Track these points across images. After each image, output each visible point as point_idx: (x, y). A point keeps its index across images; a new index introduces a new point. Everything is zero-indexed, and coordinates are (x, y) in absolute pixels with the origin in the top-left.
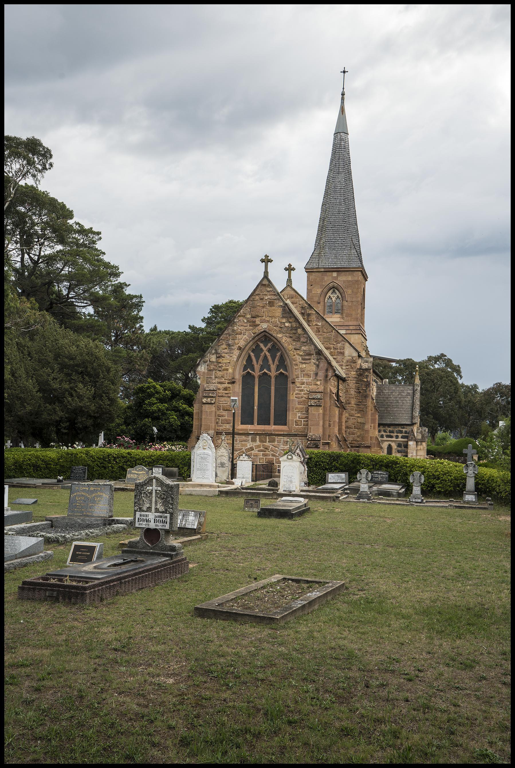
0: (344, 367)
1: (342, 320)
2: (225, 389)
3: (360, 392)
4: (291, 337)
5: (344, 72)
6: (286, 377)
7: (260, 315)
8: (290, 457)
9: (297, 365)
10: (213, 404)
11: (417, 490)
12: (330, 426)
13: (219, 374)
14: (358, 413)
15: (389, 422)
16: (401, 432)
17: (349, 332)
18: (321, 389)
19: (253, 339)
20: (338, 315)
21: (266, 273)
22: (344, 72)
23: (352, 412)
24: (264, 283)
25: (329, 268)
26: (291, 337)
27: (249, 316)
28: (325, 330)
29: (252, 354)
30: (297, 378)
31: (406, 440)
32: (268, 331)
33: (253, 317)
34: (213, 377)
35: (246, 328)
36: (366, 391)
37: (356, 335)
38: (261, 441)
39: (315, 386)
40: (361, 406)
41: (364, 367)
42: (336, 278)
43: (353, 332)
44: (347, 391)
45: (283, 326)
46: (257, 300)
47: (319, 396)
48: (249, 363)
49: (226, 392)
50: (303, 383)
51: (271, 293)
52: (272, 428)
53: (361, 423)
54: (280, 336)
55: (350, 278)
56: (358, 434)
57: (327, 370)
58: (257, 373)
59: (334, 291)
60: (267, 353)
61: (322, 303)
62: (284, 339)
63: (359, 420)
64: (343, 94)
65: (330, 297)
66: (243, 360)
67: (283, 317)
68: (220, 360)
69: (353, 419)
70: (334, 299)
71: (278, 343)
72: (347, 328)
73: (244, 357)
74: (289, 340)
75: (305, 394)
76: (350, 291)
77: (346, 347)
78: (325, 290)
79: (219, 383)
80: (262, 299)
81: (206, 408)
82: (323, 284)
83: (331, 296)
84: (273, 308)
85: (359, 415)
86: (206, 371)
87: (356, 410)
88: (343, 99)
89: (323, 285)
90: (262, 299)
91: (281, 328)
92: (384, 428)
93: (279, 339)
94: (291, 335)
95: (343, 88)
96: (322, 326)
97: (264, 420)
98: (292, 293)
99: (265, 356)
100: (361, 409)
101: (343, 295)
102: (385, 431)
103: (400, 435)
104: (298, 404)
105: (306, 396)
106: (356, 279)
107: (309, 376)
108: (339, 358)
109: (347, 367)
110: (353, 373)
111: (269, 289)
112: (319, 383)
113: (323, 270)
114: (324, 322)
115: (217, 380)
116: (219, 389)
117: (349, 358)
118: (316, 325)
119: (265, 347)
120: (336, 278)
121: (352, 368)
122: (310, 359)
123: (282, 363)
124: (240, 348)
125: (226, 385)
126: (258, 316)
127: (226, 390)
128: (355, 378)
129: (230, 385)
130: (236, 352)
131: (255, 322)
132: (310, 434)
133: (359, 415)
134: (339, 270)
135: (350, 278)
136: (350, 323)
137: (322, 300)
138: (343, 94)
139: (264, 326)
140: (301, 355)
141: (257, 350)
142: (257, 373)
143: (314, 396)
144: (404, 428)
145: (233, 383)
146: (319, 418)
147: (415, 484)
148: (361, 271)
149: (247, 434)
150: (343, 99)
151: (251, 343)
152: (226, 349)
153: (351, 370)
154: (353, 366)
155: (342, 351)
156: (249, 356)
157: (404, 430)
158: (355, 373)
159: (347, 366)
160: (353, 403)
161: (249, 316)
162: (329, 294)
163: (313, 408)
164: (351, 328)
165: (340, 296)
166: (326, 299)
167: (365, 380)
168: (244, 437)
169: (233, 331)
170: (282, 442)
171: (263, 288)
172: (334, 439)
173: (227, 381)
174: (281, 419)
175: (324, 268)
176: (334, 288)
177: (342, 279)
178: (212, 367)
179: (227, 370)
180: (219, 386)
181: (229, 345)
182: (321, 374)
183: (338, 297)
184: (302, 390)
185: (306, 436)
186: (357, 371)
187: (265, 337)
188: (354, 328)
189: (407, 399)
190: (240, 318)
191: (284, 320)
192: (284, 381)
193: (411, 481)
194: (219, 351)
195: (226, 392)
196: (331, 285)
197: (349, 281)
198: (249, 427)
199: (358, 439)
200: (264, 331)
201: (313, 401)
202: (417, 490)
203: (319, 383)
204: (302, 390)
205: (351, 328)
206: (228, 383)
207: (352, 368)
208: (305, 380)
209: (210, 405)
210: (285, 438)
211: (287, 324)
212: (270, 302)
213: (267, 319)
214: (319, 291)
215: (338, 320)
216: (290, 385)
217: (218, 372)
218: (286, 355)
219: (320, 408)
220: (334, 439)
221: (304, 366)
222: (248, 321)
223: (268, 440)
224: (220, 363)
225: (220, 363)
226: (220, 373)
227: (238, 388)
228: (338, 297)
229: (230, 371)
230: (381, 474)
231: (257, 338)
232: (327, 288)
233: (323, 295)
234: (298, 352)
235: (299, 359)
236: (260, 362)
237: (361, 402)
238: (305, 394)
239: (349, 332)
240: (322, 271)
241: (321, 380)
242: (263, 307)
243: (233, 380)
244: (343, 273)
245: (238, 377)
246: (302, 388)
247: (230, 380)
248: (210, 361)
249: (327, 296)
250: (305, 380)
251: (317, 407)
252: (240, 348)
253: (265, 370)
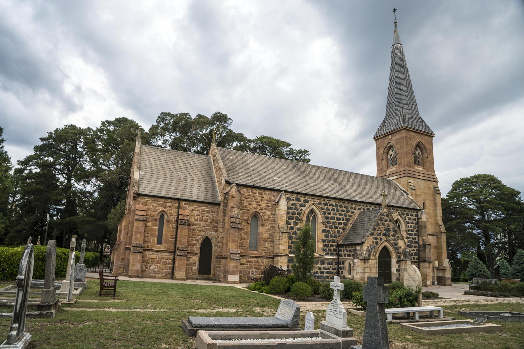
5: (395, 10)
15: (348, 243)
17: (399, 176)
22: (395, 10)
37: (404, 178)
42: (391, 139)
43: (402, 176)
55: (398, 137)
72: (398, 174)
76: (399, 146)
78: (386, 150)
106: (402, 136)
120: (391, 139)
135: (398, 137)
137: (385, 157)
162: (390, 152)
164: (401, 173)
166: (389, 156)
175: (383, 135)
188: (403, 172)
196: (389, 145)
197: (398, 139)
205: (401, 173)
239: (399, 176)
244: (394, 134)
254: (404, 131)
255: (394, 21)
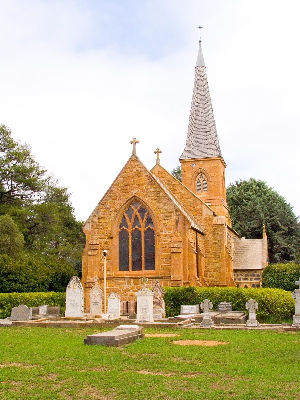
0: (203, 224)
1: (209, 196)
2: (106, 243)
3: (216, 243)
4: (156, 200)
5: (200, 28)
6: (153, 232)
7: (131, 184)
8: (144, 292)
9: (161, 221)
10: (96, 255)
11: (252, 316)
12: (189, 269)
13: (101, 231)
14: (216, 259)
16: (254, 275)
18: (181, 239)
19: (127, 202)
20: (206, 192)
21: (134, 151)
22: (200, 28)
23: (211, 259)
24: (133, 159)
25: (197, 159)
26: (156, 200)
27: (122, 185)
28: (187, 197)
29: (126, 215)
30: (161, 231)
31: (258, 281)
32: (137, 196)
33: (126, 186)
34: (97, 234)
35: (121, 194)
36: (221, 242)
37: (219, 206)
38: (135, 283)
39: (176, 237)
40: (218, 254)
41: (218, 224)
44: (206, 243)
45: (149, 191)
46: (128, 173)
47: (179, 245)
48: (124, 223)
49: (107, 245)
50: (166, 236)
51: (139, 167)
52: (143, 272)
53: (218, 267)
54: (147, 199)
56: (217, 276)
57: (185, 225)
58: (130, 230)
59: (202, 175)
60: (138, 214)
61: (193, 184)
62: (150, 202)
63: (217, 265)
64: (200, 42)
65: (199, 180)
66: (119, 220)
67: (149, 184)
68: (102, 221)
69: (211, 264)
70: (202, 181)
71: (145, 205)
72: (212, 201)
73: (119, 218)
74: (154, 202)
75: (168, 244)
77: (203, 209)
78: (195, 175)
79: (101, 239)
80: (132, 172)
81: (90, 259)
82: (194, 170)
83: (200, 179)
84: (141, 178)
85: (216, 261)
86: (91, 230)
87: (214, 257)
88: (200, 45)
89: (193, 171)
90: (132, 172)
91: (147, 193)
92: (241, 273)
93: (146, 202)
94: (155, 198)
95: (200, 38)
96: (185, 193)
97: (137, 266)
98: (161, 170)
99: (136, 216)
100: (218, 256)
101: (208, 178)
102: (242, 275)
103: (253, 278)
104: (163, 253)
105: (169, 246)
106: (217, 165)
107: (170, 229)
108: (199, 217)
109: (205, 224)
110: (210, 228)
111: (137, 164)
112: (179, 234)
113: (192, 160)
114: (186, 191)
115: (99, 236)
116: (101, 244)
117: (206, 217)
118: (180, 193)
119: (136, 208)
120: (202, 166)
121: (209, 225)
122: (171, 216)
123: (149, 221)
124: (116, 211)
125: (107, 240)
126: (129, 185)
127: (106, 244)
128: (212, 232)
129: (109, 240)
130: (114, 214)
131: (127, 189)
132: (173, 277)
133: (216, 261)
134: (204, 160)
136: (215, 198)
137: (193, 182)
138: (200, 42)
139: (134, 192)
140: (164, 213)
141: (129, 211)
142: (130, 230)
143: (176, 245)
144: (256, 272)
145: (112, 238)
146: (180, 262)
147: (250, 311)
148: (220, 160)
149: (124, 279)
150: (200, 45)
151: (125, 206)
152: (105, 211)
153: (209, 226)
154: (209, 223)
155: (201, 212)
156: (124, 217)
157: (256, 274)
158: (211, 228)
159: (205, 223)
160: (211, 251)
161: (122, 185)
163: (175, 254)
164: (215, 201)
165: (206, 179)
166: (196, 181)
167: (220, 233)
168: (121, 281)
169: (111, 197)
170: (152, 283)
171: (132, 163)
172: (193, 279)
173: (107, 237)
174: (151, 264)
176: (201, 173)
177: (206, 167)
178: (95, 226)
179: (107, 228)
180: (101, 241)
181: (107, 208)
182: (180, 226)
183: (205, 179)
184: (165, 241)
185: (170, 278)
186: (213, 227)
187: (135, 200)
189: (258, 250)
190: (115, 187)
191: (149, 187)
192: (151, 234)
193: (247, 308)
194: (100, 214)
195: (107, 245)
196: (199, 171)
198: (125, 272)
199: (217, 280)
200: (134, 196)
201: (174, 249)
202: (252, 316)
203: (179, 234)
204: (165, 241)
205: (215, 201)
206: (108, 238)
207: (209, 225)
208: (168, 232)
209: (94, 257)
210: (153, 280)
211: (152, 190)
212: (138, 174)
213: (137, 186)
214: (191, 176)
215: (206, 196)
216: (156, 238)
217: (100, 230)
218: (152, 214)
219: (180, 254)
220: (193, 279)
221: (166, 221)
222: (122, 189)
223: (140, 283)
224: (101, 223)
225: (101, 223)
226: (102, 230)
227: (116, 241)
228: (205, 179)
229: (109, 228)
230: (226, 305)
231: (129, 202)
232: (197, 173)
233: (194, 179)
234: (161, 211)
235: (162, 216)
236: (133, 220)
237: (217, 251)
238: (168, 244)
240: (192, 161)
241: (180, 232)
242: (133, 178)
243: (112, 236)
244: (207, 162)
245: (116, 233)
246: (166, 240)
247: (109, 236)
248: (94, 222)
249: (197, 179)
250: (168, 232)
251: (178, 254)
252: (116, 211)
253: (137, 227)
254: (220, 161)
255: (199, 40)
